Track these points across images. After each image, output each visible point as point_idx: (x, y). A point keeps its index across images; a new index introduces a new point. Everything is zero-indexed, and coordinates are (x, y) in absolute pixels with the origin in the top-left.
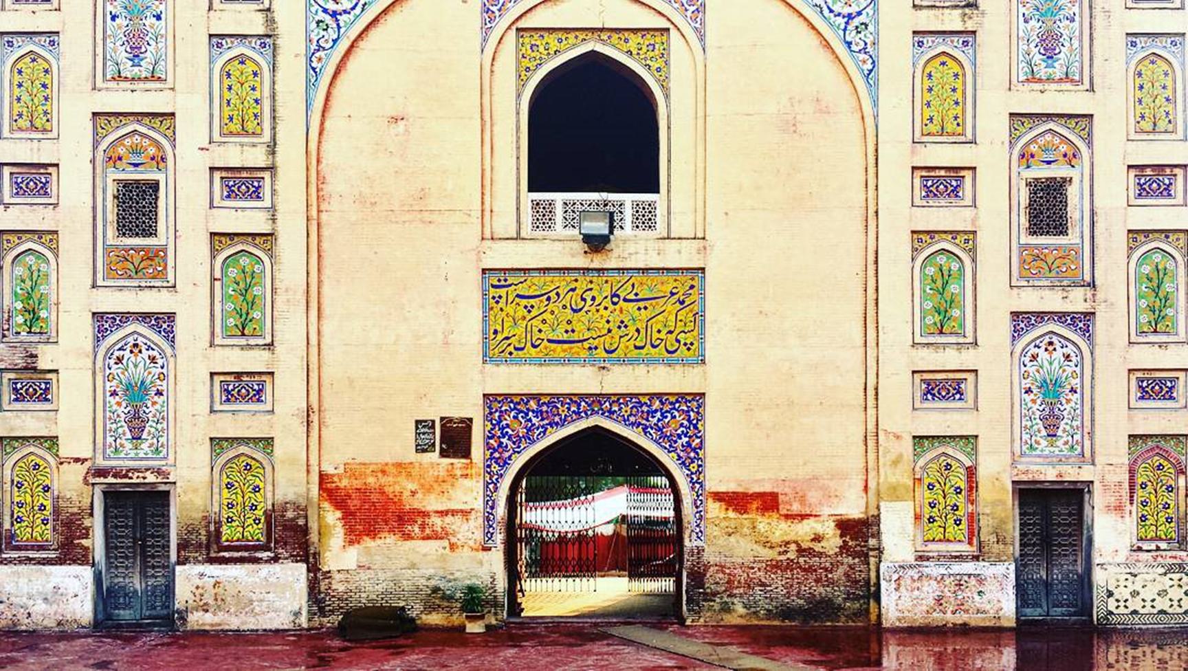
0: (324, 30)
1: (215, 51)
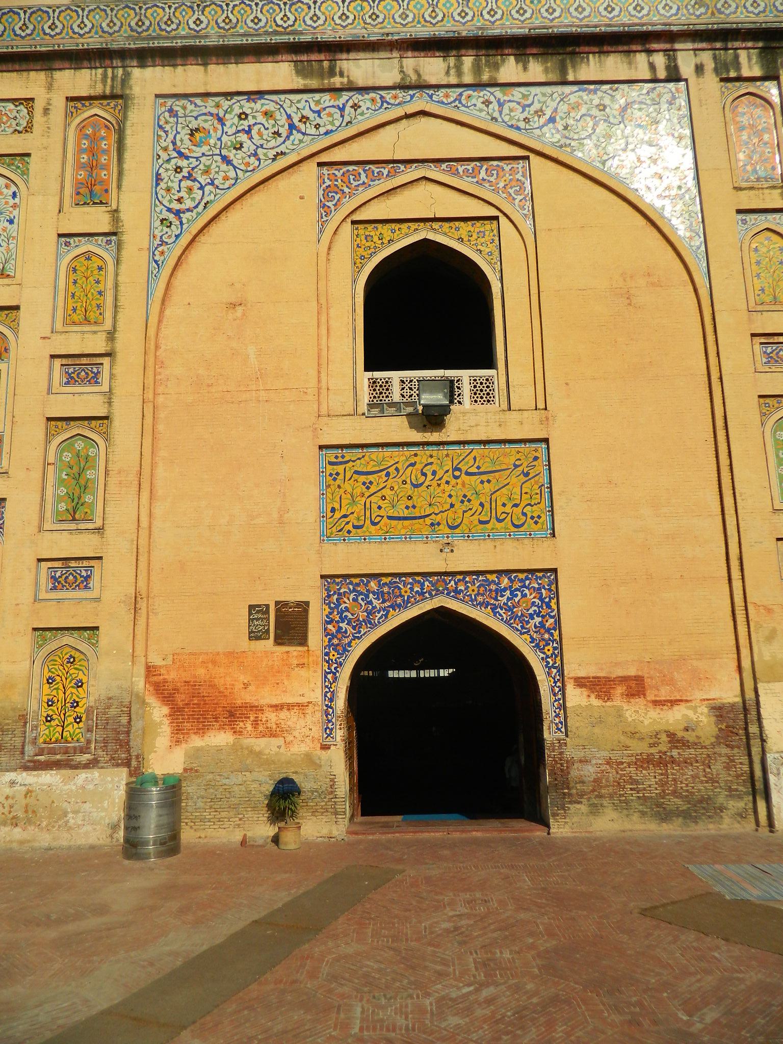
0: (168, 227)
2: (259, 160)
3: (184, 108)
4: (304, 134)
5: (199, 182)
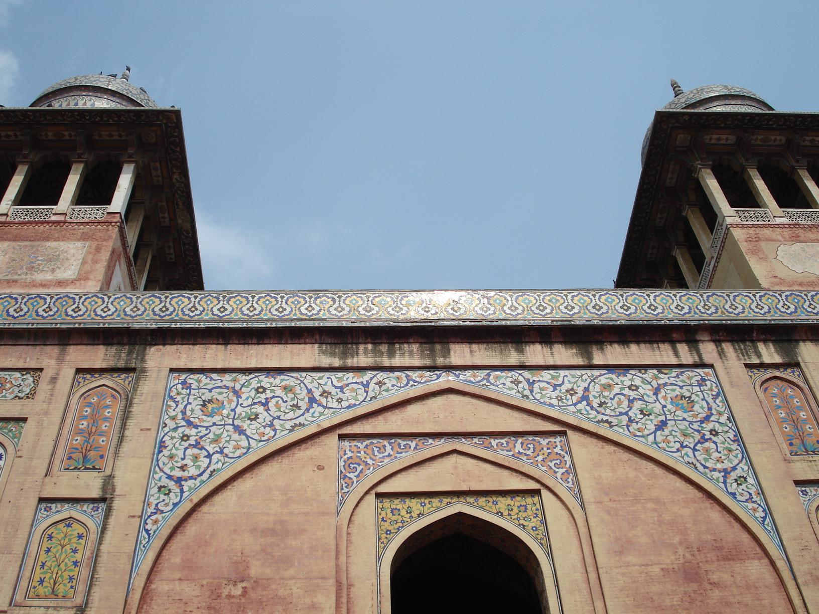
0: (165, 494)
1: (42, 514)
2: (275, 430)
3: (199, 381)
4: (325, 407)
5: (207, 451)
